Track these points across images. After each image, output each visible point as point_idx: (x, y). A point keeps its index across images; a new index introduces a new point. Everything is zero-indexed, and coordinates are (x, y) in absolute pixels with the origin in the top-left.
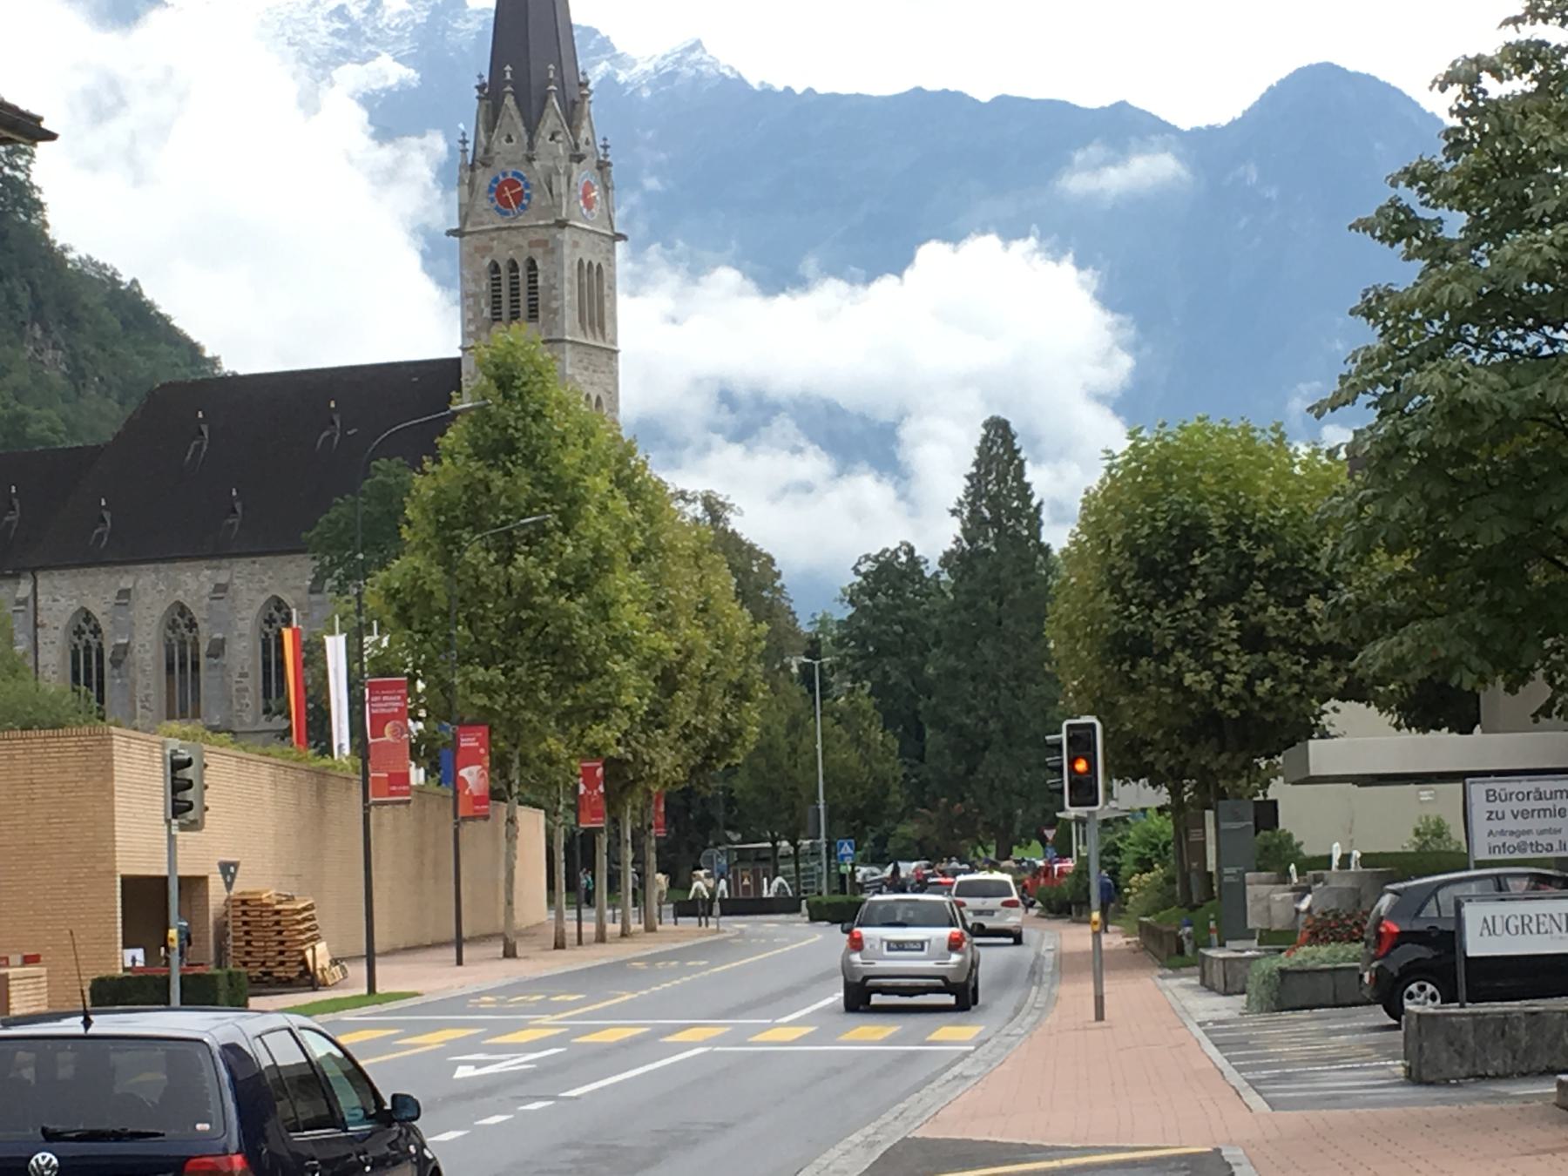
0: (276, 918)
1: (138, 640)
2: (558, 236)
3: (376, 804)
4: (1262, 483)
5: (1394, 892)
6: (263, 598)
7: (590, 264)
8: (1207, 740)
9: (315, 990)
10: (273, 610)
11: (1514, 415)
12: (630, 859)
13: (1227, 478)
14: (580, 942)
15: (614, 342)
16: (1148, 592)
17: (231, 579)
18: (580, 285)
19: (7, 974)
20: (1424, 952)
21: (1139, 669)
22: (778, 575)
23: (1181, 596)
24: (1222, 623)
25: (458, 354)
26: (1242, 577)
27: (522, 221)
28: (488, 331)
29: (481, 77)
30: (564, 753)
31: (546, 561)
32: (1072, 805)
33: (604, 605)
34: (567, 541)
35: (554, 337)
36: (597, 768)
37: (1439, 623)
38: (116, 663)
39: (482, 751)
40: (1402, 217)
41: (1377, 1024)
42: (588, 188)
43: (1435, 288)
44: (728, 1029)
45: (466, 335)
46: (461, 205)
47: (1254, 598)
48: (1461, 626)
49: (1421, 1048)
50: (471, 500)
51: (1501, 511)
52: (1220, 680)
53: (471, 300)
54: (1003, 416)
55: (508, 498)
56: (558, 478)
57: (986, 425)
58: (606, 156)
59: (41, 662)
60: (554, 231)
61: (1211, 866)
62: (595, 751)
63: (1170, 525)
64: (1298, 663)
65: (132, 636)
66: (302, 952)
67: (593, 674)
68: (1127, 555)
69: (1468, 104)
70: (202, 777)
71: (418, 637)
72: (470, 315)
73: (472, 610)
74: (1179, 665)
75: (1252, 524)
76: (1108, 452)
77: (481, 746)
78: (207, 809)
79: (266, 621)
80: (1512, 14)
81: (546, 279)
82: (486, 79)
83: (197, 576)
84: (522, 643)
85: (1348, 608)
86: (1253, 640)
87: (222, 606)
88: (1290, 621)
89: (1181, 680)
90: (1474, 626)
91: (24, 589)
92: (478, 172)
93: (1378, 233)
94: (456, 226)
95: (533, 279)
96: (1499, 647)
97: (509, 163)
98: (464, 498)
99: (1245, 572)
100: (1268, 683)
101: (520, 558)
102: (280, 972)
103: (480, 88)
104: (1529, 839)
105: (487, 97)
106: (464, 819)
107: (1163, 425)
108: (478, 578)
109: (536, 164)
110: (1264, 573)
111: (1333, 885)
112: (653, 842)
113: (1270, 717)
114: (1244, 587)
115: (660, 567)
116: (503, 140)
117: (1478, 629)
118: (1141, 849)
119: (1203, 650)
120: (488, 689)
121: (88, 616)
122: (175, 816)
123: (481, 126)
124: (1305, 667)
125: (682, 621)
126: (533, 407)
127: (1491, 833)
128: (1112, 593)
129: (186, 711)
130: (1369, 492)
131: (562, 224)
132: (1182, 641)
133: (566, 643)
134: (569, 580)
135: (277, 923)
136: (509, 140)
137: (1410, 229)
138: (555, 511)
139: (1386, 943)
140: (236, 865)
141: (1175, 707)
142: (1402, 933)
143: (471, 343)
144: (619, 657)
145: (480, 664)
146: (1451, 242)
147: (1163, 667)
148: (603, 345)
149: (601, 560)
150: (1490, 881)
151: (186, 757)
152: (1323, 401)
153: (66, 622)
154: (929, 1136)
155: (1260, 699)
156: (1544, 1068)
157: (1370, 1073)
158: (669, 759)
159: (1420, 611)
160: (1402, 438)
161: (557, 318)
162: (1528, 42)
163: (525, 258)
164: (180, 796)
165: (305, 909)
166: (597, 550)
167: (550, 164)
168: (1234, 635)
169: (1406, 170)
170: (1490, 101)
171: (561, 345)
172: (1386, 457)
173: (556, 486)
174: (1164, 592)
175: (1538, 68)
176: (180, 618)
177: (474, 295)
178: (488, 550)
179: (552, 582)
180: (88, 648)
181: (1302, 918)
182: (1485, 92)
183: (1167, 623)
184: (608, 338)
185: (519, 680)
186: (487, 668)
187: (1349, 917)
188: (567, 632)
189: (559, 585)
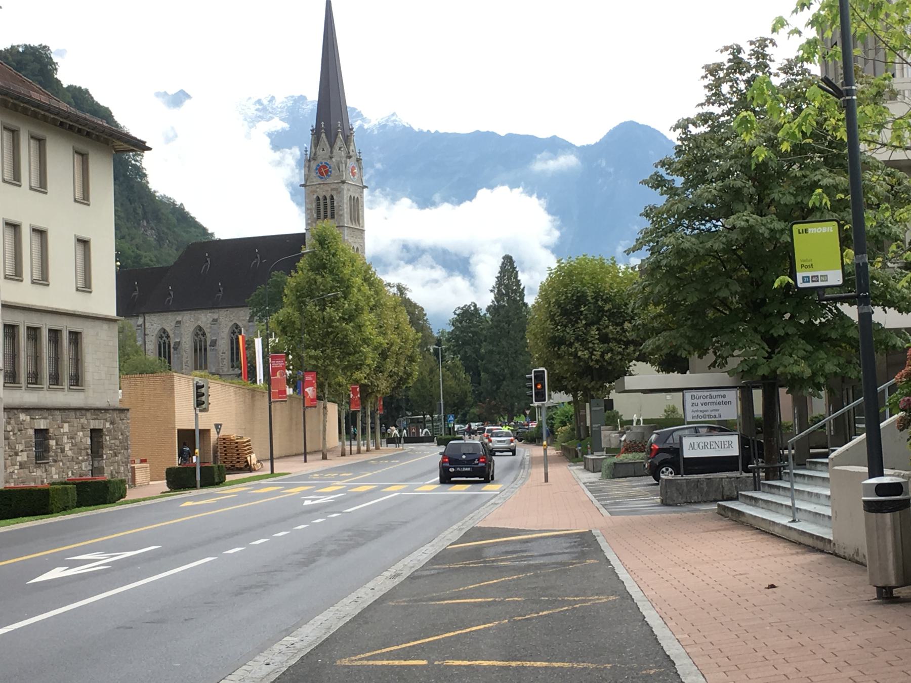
0: (236, 445)
1: (184, 340)
2: (342, 187)
3: (274, 402)
4: (607, 279)
5: (657, 433)
6: (231, 324)
7: (354, 197)
8: (587, 376)
9: (251, 472)
10: (234, 329)
11: (701, 254)
12: (370, 422)
13: (593, 278)
14: (351, 454)
15: (363, 227)
16: (565, 321)
18: (350, 205)
19: (134, 467)
20: (667, 456)
21: (561, 350)
22: (425, 315)
23: (578, 323)
24: (592, 332)
26: (600, 315)
27: (328, 181)
28: (316, 223)
29: (312, 126)
30: (344, 382)
31: (337, 310)
32: (536, 401)
33: (359, 326)
34: (346, 302)
36: (357, 388)
37: (672, 333)
38: (175, 349)
39: (314, 382)
40: (659, 179)
41: (650, 483)
42: (353, 168)
43: (672, 206)
44: (405, 486)
45: (307, 224)
46: (305, 175)
47: (604, 323)
48: (681, 333)
49: (667, 492)
50: (309, 287)
51: (696, 290)
52: (592, 354)
53: (309, 212)
54: (510, 255)
55: (324, 286)
56: (342, 278)
57: (504, 258)
58: (360, 156)
59: (146, 349)
60: (341, 184)
61: (588, 424)
62: (357, 382)
63: (573, 296)
64: (621, 347)
65: (181, 338)
66: (246, 458)
67: (356, 352)
68: (557, 307)
69: (684, 136)
70: (208, 392)
71: (290, 338)
72: (309, 217)
73: (310, 328)
74: (576, 348)
75: (603, 295)
76: (549, 268)
77: (313, 380)
78: (210, 404)
80: (700, 102)
81: (337, 203)
82: (315, 127)
84: (329, 341)
85: (639, 327)
86: (604, 339)
87: (215, 327)
88: (618, 331)
89: (577, 354)
90: (686, 332)
91: (140, 321)
92: (312, 162)
93: (650, 185)
95: (332, 203)
96: (696, 341)
97: (323, 159)
98: (307, 286)
99: (601, 313)
100: (609, 355)
101: (328, 308)
102: (238, 465)
103: (312, 131)
104: (707, 413)
105: (315, 134)
106: (307, 407)
107: (570, 258)
108: (312, 316)
109: (333, 159)
110: (608, 314)
111: (633, 431)
112: (378, 416)
113: (610, 368)
114: (600, 319)
115: (381, 312)
116: (321, 150)
117: (688, 334)
118: (562, 418)
119: (585, 343)
120: (316, 358)
121: (164, 331)
122: (197, 406)
124: (624, 349)
125: (389, 332)
126: (333, 251)
127: (693, 411)
128: (551, 321)
130: (647, 283)
131: (343, 182)
132: (577, 339)
133: (345, 340)
134: (346, 317)
135: (237, 447)
136: (323, 150)
137: (663, 183)
138: (342, 291)
139: (653, 454)
140: (221, 425)
141: (575, 364)
142: (659, 449)
143: (309, 227)
144: (365, 346)
145: (313, 349)
146: (677, 188)
147: (570, 349)
148: (358, 228)
149: (358, 310)
150: (693, 429)
151: (202, 384)
152: (629, 249)
153: (156, 332)
154: (482, 526)
155: (606, 361)
156: (712, 500)
157: (647, 502)
158: (384, 384)
159: (666, 328)
160: (659, 262)
161: (342, 218)
162: (706, 113)
164: (199, 399)
165: (247, 441)
166: (357, 305)
167: (339, 159)
168: (597, 337)
169: (661, 161)
170: (692, 135)
172: (653, 270)
173: (341, 281)
174: (570, 321)
175: (710, 123)
176: (200, 332)
177: (311, 209)
178: (316, 306)
179: (340, 317)
180: (164, 343)
181: (622, 444)
182: (690, 132)
183: (571, 332)
184: (361, 225)
185: (328, 355)
186: (315, 350)
187: (640, 443)
188: (346, 336)
189: (342, 319)
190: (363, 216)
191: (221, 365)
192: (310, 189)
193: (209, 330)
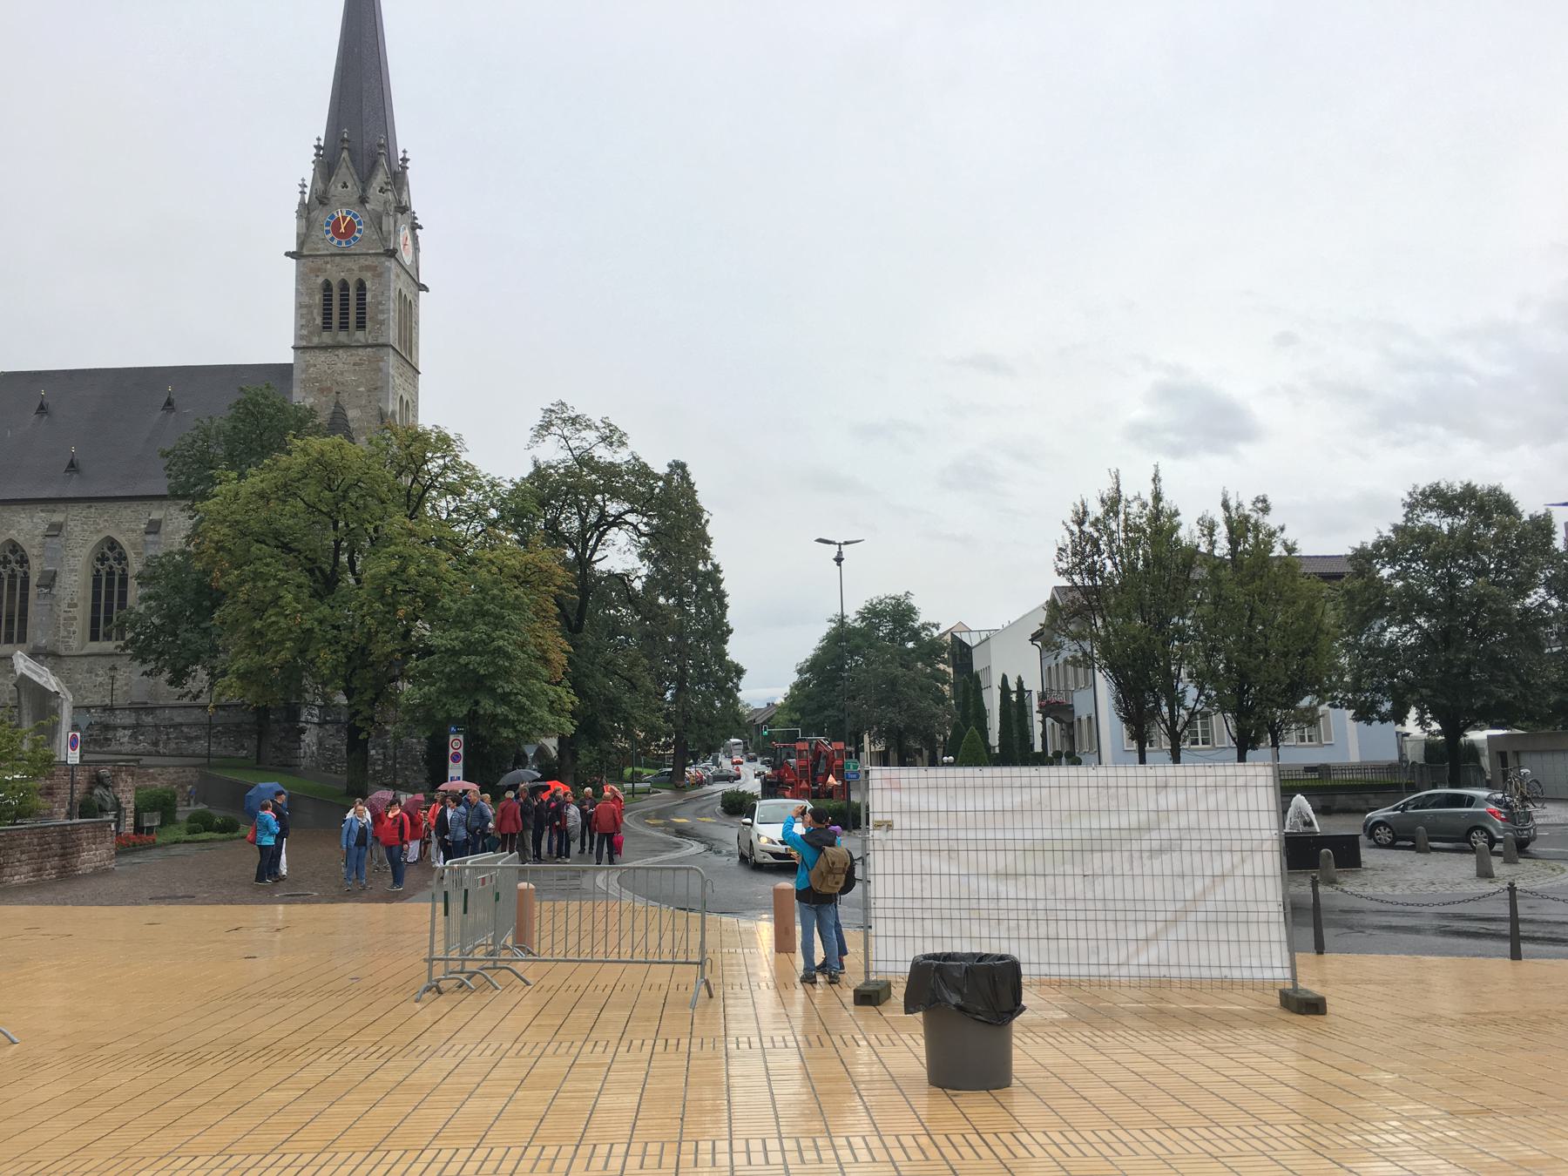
6: (96, 538)
10: (106, 550)
17: (66, 521)
18: (400, 311)
25: (288, 357)
29: (319, 139)
35: (381, 341)
45: (298, 337)
46: (298, 236)
57: (670, 466)
60: (383, 259)
72: (303, 322)
79: (98, 559)
82: (322, 144)
83: (32, 517)
94: (293, 248)
97: (344, 205)
103: (318, 147)
116: (339, 185)
123: (318, 175)
129: (12, 635)
136: (345, 186)
163: (355, 279)
171: (385, 349)
177: (309, 306)
184: (414, 360)
190: (417, 343)
191: (63, 633)
192: (309, 262)
193: (35, 551)
